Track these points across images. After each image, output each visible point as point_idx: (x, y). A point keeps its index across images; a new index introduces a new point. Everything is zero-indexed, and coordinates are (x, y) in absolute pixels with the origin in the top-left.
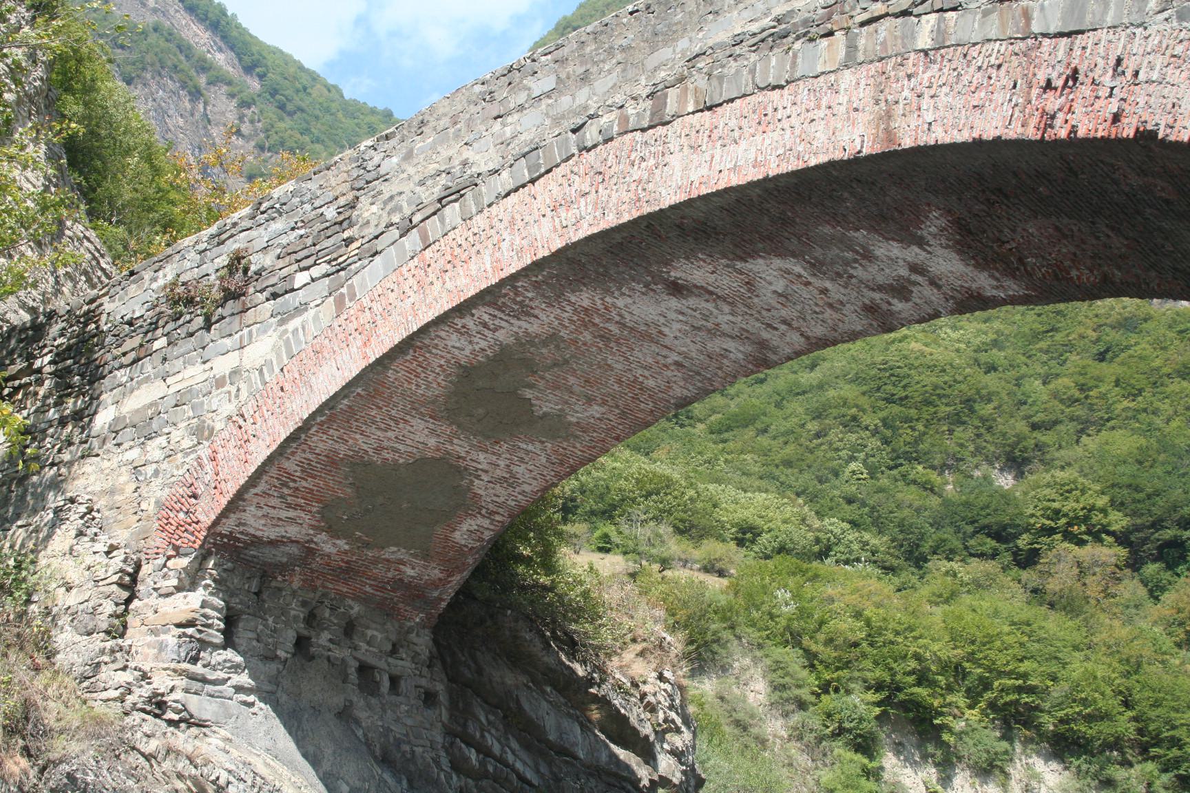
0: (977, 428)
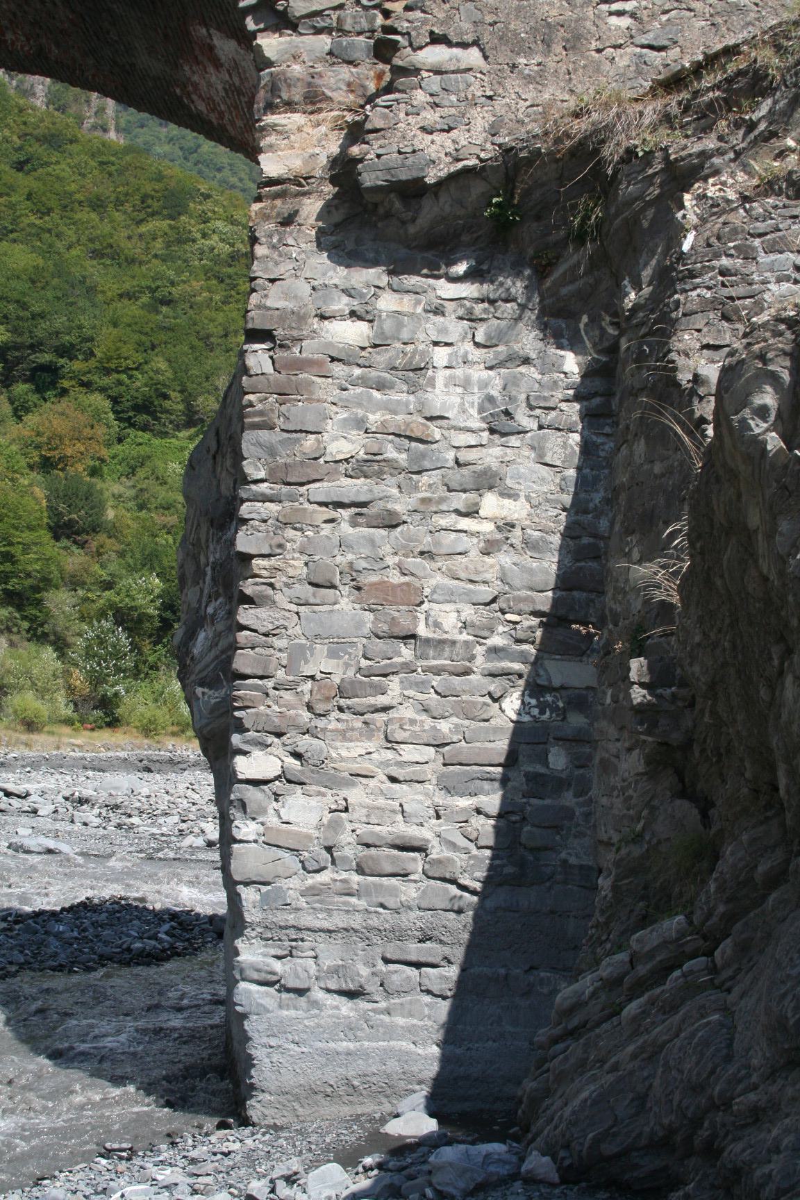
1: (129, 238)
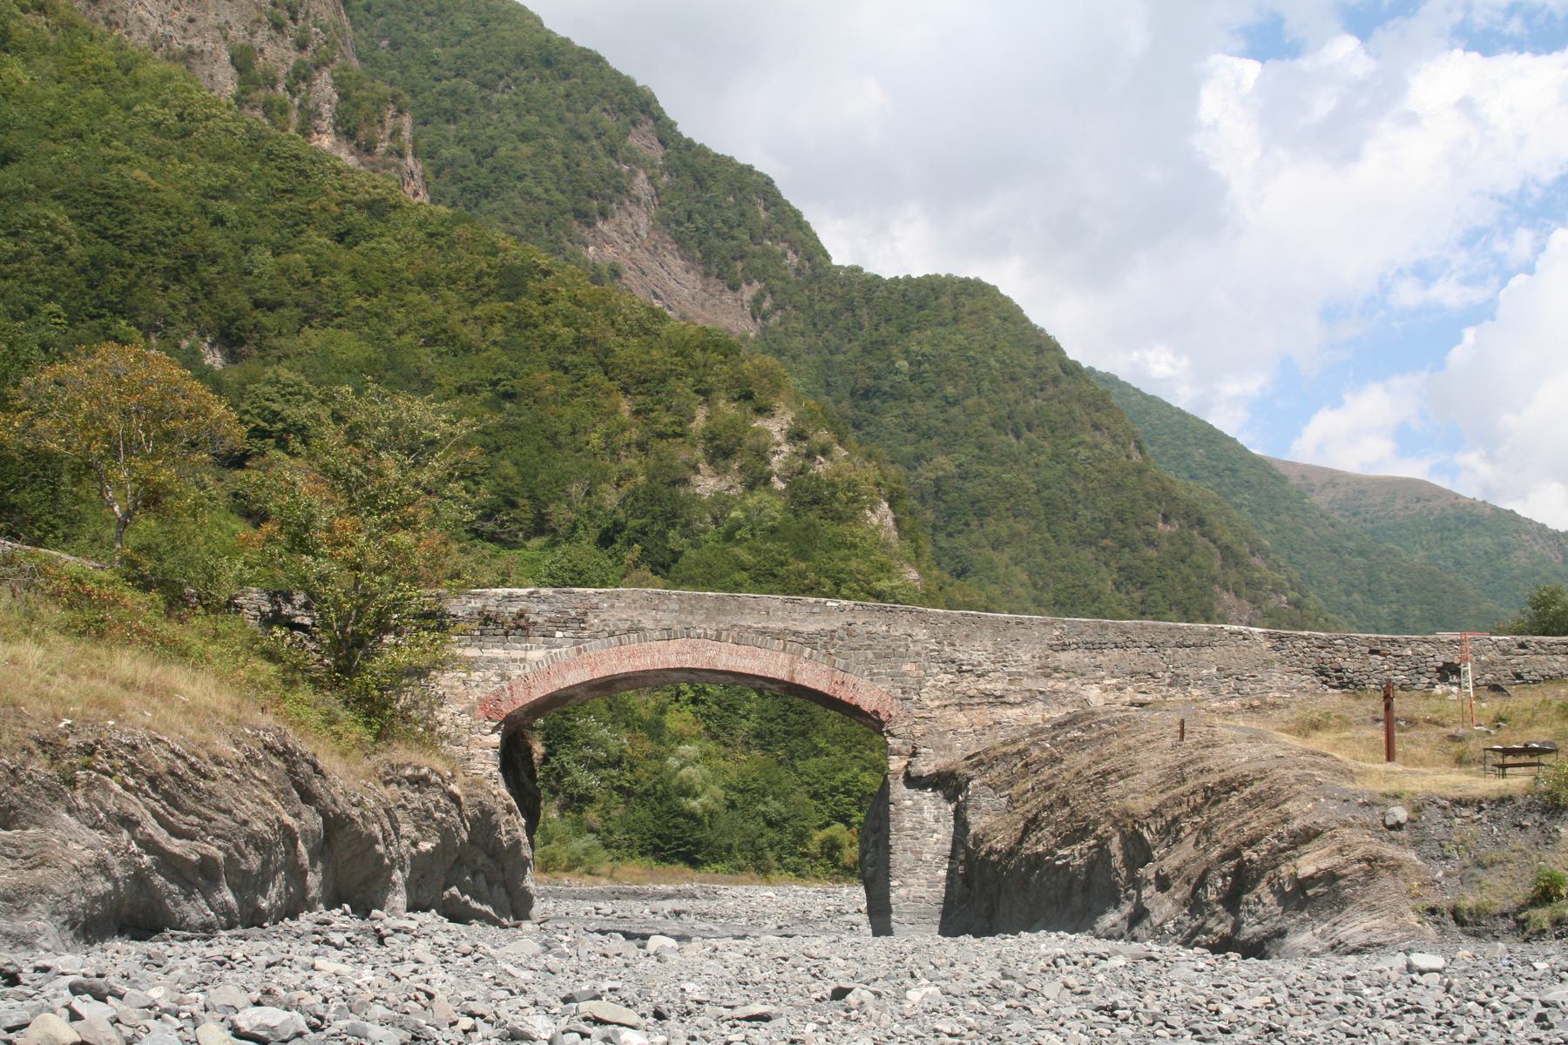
0: (194, 290)
1: (464, 321)
